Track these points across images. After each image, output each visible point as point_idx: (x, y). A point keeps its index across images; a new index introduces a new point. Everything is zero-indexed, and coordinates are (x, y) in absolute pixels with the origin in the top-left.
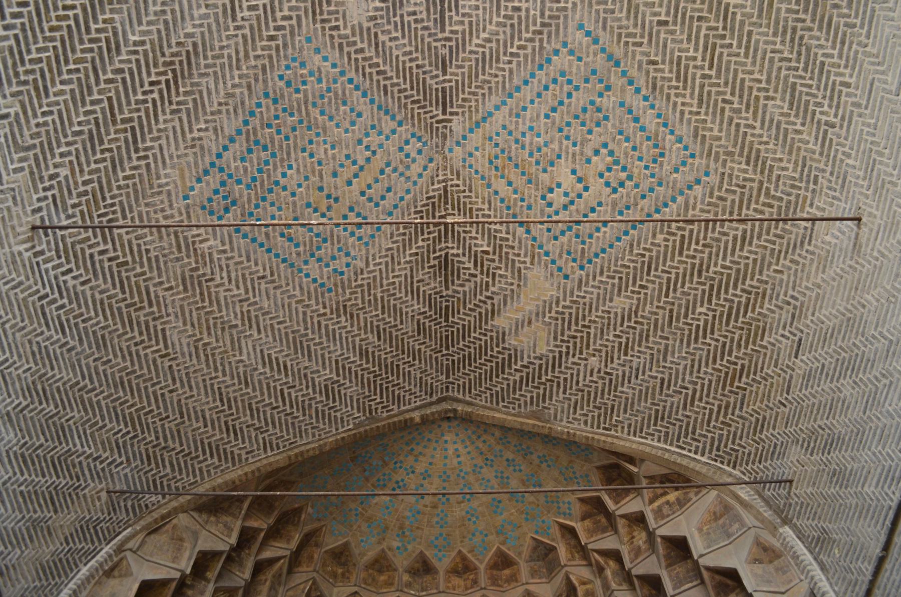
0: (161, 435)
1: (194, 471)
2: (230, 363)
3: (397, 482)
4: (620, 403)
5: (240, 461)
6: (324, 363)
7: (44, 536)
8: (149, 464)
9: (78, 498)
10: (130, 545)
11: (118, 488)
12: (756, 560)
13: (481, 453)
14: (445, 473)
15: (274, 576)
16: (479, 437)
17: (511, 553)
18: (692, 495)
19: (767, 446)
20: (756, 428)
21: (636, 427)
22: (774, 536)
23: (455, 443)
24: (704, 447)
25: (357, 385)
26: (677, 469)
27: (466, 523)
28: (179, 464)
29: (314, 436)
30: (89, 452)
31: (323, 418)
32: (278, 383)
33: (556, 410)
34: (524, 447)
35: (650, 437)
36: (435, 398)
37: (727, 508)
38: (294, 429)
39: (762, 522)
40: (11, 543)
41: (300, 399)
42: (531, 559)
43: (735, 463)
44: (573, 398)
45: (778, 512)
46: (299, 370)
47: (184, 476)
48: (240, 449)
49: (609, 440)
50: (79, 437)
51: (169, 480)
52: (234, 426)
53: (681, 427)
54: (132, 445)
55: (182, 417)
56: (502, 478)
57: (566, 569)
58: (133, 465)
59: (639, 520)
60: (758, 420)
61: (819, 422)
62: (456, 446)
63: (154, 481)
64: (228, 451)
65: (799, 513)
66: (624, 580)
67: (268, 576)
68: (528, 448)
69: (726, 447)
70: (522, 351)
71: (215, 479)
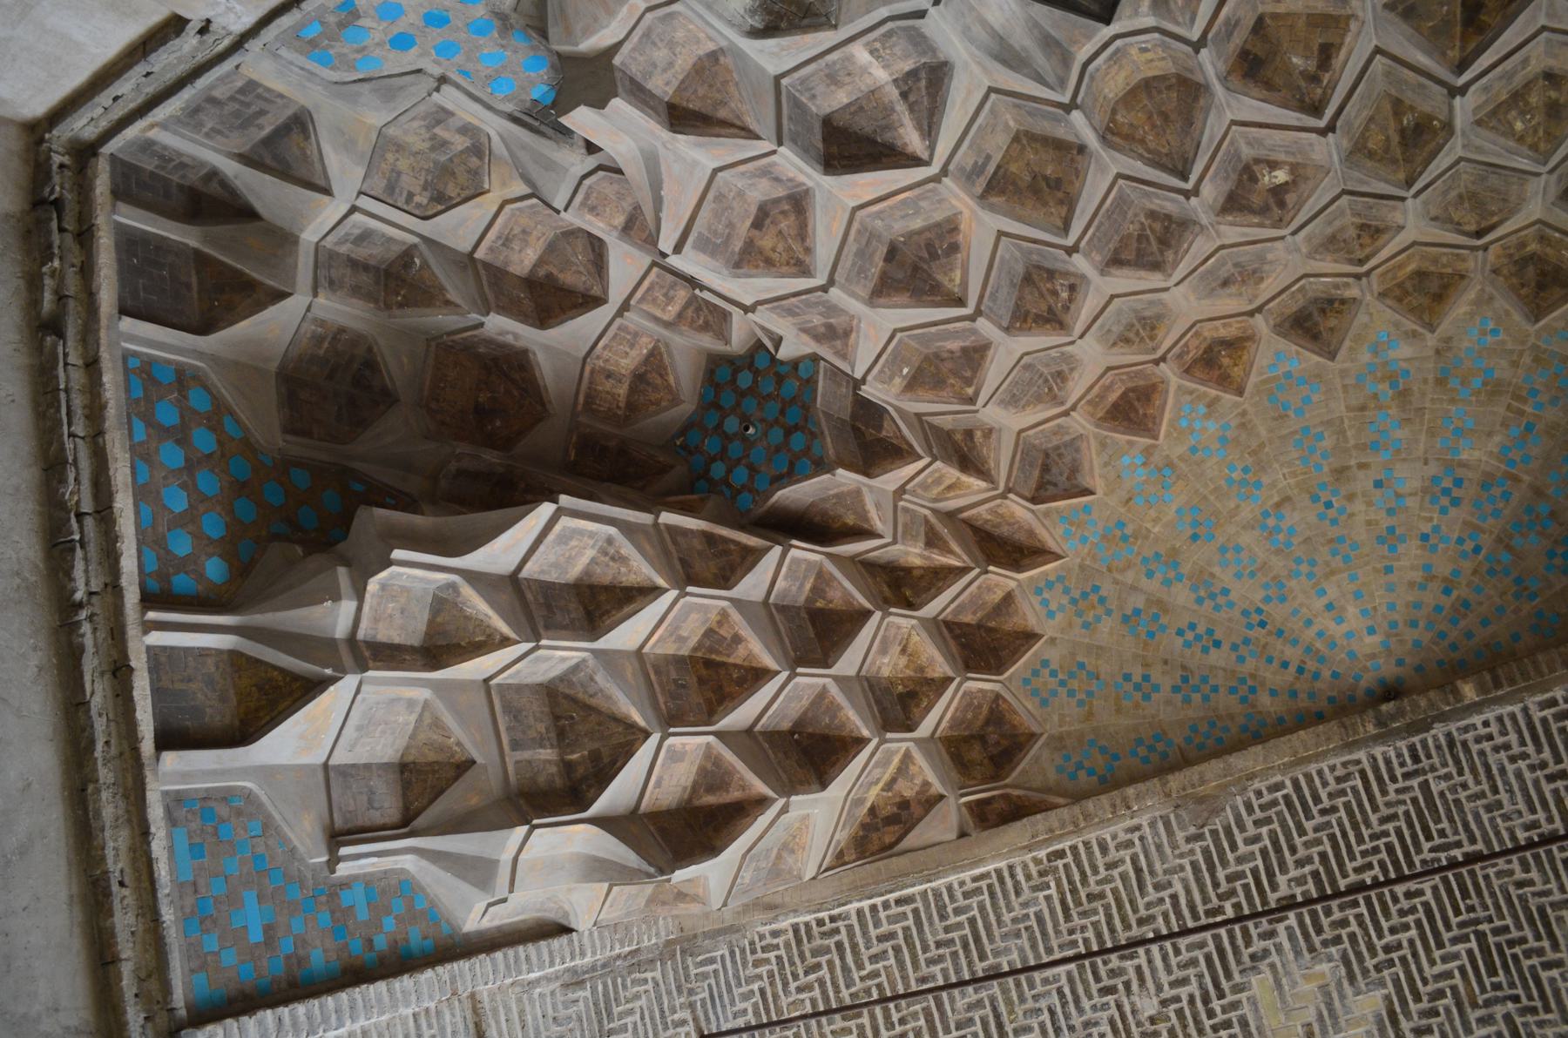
3: (1456, 502)
4: (1058, 932)
13: (1280, 633)
14: (1346, 559)
16: (1300, 670)
24: (865, 933)
26: (896, 863)
27: (1249, 460)
33: (1174, 846)
34: (1196, 697)
35: (970, 886)
36: (1439, 730)
42: (1074, 444)
43: (799, 942)
44: (1152, 895)
53: (925, 949)
56: (1212, 596)
62: (1344, 628)
68: (1187, 701)
69: (830, 963)
70: (1298, 953)
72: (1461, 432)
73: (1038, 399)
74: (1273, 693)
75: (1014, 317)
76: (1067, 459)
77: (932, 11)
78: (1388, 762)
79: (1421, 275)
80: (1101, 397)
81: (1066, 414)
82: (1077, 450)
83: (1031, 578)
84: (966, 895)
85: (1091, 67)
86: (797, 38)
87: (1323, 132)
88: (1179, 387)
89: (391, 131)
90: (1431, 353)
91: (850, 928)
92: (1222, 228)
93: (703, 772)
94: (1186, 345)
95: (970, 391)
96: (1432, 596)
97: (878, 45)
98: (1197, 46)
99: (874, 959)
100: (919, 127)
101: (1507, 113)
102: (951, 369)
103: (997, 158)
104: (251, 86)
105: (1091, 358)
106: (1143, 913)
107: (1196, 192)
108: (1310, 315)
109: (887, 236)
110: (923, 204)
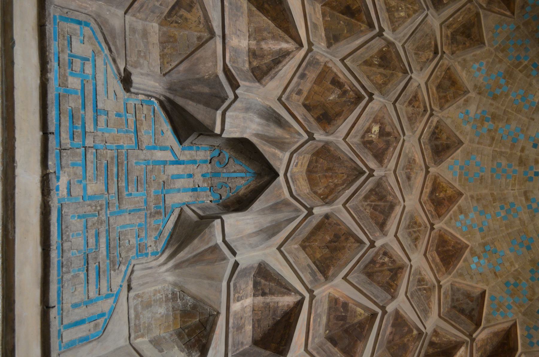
17: (461, 264)
27: (497, 204)
42: (454, 290)
73: (428, 298)
75: (388, 291)
76: (461, 297)
77: (237, 258)
79: (439, 87)
80: (436, 265)
81: (440, 287)
82: (458, 290)
83: (523, 345)
85: (294, 193)
86: (215, 337)
87: (371, 99)
88: (446, 223)
90: (479, 96)
92: (389, 167)
94: (429, 211)
95: (415, 332)
97: (237, 295)
98: (311, 137)
100: (283, 294)
101: (395, 17)
103: (310, 262)
105: (418, 261)
107: (372, 171)
108: (436, 145)
109: (323, 339)
110: (318, 312)
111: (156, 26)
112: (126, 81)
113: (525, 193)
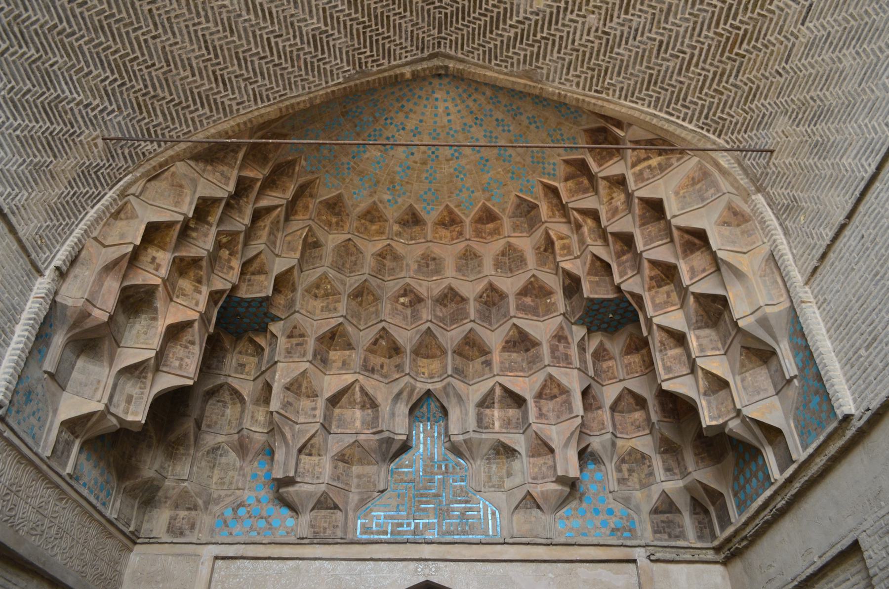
0: (149, 83)
1: (186, 121)
2: (212, 8)
4: (615, 65)
5: (231, 112)
6: (311, 11)
7: (48, 180)
8: (141, 113)
9: (75, 144)
10: (132, 190)
11: (113, 135)
12: (725, 223)
14: (435, 130)
15: (272, 223)
17: (496, 209)
18: (674, 160)
19: (755, 116)
20: (747, 97)
21: (628, 91)
22: (746, 202)
23: (445, 101)
24: (693, 115)
25: (346, 36)
26: (663, 135)
28: (171, 114)
29: (304, 88)
30: (78, 99)
31: (313, 70)
32: (264, 32)
33: (549, 70)
34: (514, 107)
35: (640, 102)
36: (426, 54)
37: (705, 174)
38: (283, 80)
39: (737, 189)
40: (17, 185)
41: (288, 49)
42: (514, 215)
43: (721, 131)
45: (754, 180)
46: (285, 17)
47: (177, 125)
48: (230, 100)
49: (600, 103)
50: (67, 83)
51: (162, 129)
52: (222, 75)
53: (673, 92)
54: (121, 93)
55: (168, 65)
57: (546, 225)
58: (125, 114)
59: (620, 182)
60: (751, 88)
61: (812, 93)
62: (447, 104)
63: (148, 130)
64: (219, 101)
65: (774, 182)
66: (600, 237)
67: (267, 222)
68: (518, 108)
69: (714, 115)
70: (518, 6)
71: (210, 130)
72: (378, 163)
74: (484, 94)
78: (451, 47)
84: (644, 100)
89: (638, 487)
91: (698, 120)
93: (692, 252)
96: (409, 106)
99: (696, 104)
102: (534, 290)
104: (655, 532)
106: (575, 53)
111: (354, 468)
112: (382, 492)
113: (447, 160)
